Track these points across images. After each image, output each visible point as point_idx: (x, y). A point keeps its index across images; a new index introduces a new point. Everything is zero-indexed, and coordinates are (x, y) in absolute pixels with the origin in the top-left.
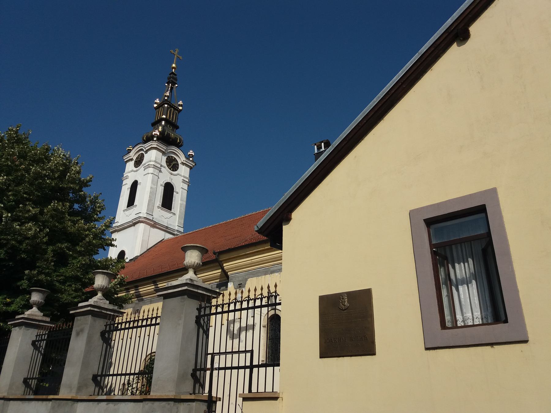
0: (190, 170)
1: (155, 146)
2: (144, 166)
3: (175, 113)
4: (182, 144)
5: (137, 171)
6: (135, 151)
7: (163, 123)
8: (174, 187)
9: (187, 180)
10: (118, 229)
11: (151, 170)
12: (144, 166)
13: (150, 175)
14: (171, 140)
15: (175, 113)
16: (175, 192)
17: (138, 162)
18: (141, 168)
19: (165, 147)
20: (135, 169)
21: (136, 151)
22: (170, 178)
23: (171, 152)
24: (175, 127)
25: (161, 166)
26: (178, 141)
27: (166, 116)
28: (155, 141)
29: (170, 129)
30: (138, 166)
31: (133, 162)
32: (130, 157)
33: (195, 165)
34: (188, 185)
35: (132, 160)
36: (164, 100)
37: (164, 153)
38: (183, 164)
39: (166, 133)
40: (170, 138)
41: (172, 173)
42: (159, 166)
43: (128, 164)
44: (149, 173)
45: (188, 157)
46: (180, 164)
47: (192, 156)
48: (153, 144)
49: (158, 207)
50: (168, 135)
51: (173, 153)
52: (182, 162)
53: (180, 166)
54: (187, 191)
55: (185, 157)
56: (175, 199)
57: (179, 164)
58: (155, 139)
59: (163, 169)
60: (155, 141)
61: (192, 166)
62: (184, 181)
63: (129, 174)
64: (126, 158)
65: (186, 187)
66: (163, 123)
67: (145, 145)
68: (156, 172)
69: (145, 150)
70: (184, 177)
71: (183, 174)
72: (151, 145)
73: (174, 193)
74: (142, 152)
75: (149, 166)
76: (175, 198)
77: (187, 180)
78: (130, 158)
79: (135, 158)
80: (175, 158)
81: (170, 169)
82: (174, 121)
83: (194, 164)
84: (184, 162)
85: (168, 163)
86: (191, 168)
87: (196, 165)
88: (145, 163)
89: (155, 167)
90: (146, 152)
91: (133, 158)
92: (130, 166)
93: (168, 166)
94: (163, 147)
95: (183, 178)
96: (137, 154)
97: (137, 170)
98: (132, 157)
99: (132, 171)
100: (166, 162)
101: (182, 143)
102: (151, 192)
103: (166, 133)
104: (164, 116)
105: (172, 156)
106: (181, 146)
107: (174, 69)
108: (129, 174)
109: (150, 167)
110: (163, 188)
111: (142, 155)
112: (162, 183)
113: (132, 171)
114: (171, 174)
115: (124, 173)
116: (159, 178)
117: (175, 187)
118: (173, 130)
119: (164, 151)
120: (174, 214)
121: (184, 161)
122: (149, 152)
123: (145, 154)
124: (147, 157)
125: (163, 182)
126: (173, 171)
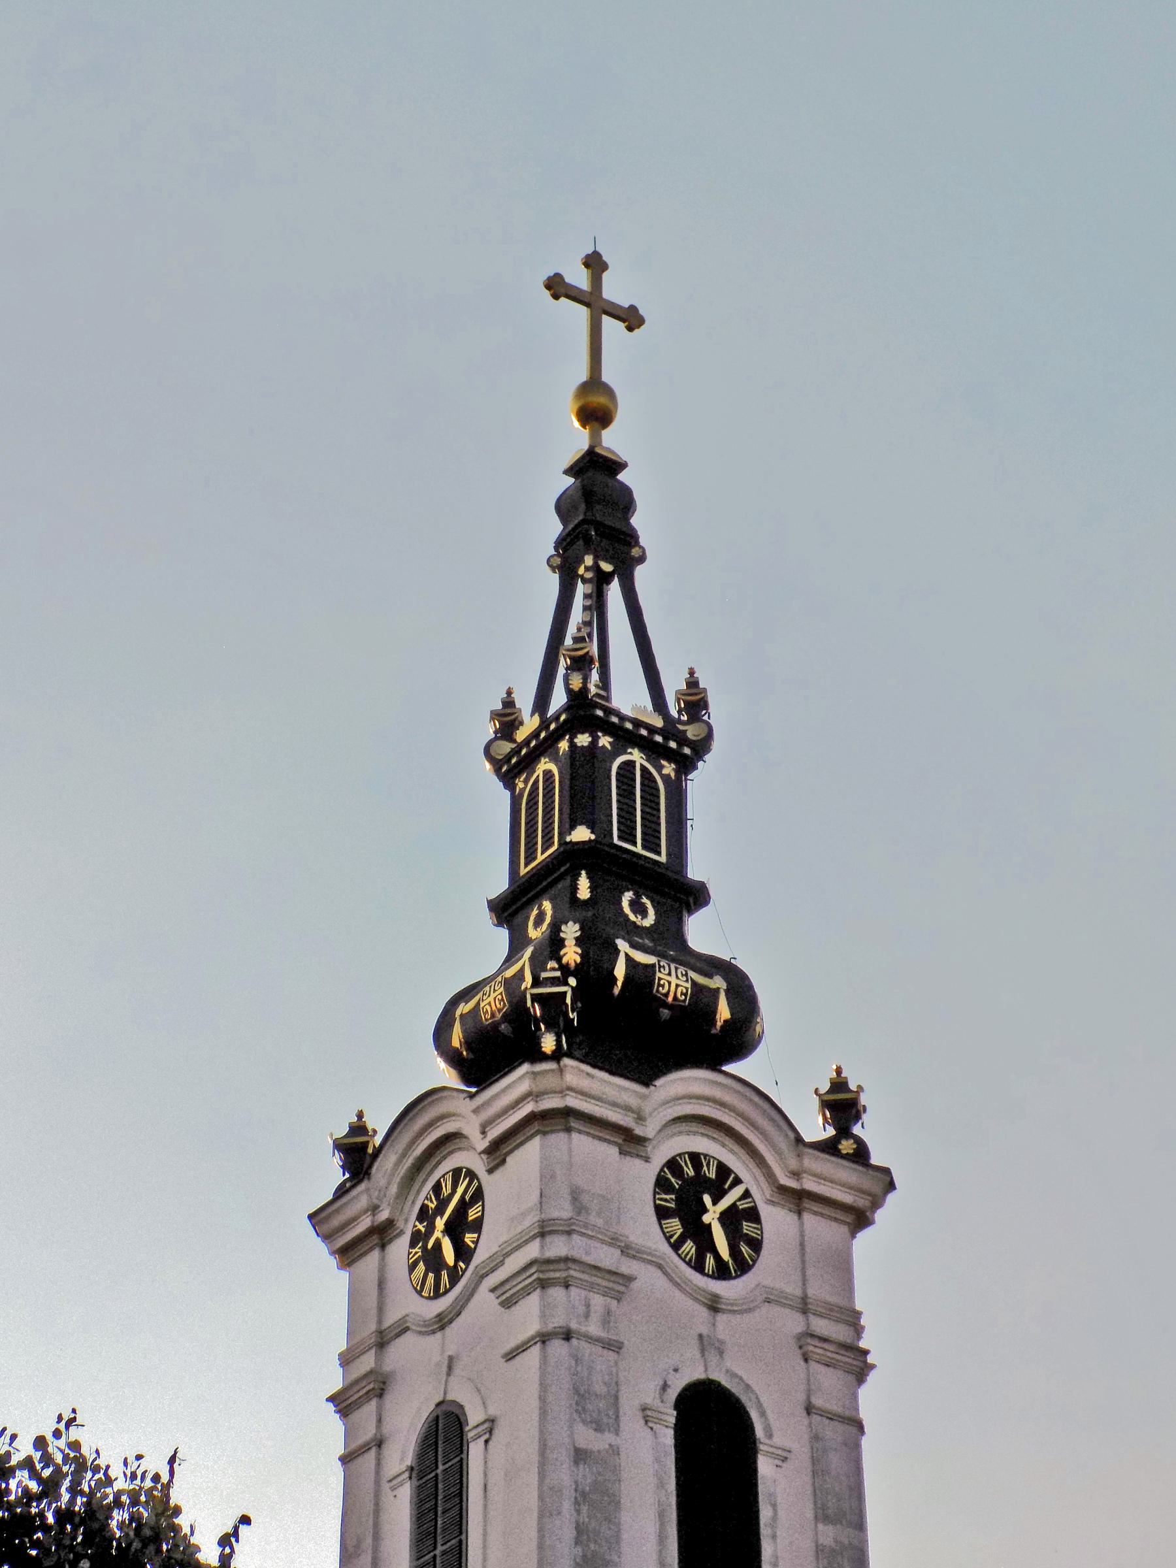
5: (442, 1322)
6: (404, 1155)
8: (754, 1415)
14: (665, 1013)
21: (409, 1161)
23: (684, 1127)
25: (628, 1251)
26: (724, 1012)
28: (557, 1055)
39: (620, 971)
46: (771, 1202)
51: (694, 1127)
52: (783, 1190)
56: (775, 1517)
57: (765, 1211)
58: (548, 1043)
60: (557, 1055)
69: (482, 1144)
73: (764, 1466)
76: (774, 1506)
88: (495, 1249)
96: (422, 1176)
97: (440, 1317)
100: (662, 1213)
102: (584, 1495)
103: (620, 971)
110: (668, 1437)
112: (651, 1398)
117: (763, 1414)
123: (490, 1171)
125: (665, 1387)
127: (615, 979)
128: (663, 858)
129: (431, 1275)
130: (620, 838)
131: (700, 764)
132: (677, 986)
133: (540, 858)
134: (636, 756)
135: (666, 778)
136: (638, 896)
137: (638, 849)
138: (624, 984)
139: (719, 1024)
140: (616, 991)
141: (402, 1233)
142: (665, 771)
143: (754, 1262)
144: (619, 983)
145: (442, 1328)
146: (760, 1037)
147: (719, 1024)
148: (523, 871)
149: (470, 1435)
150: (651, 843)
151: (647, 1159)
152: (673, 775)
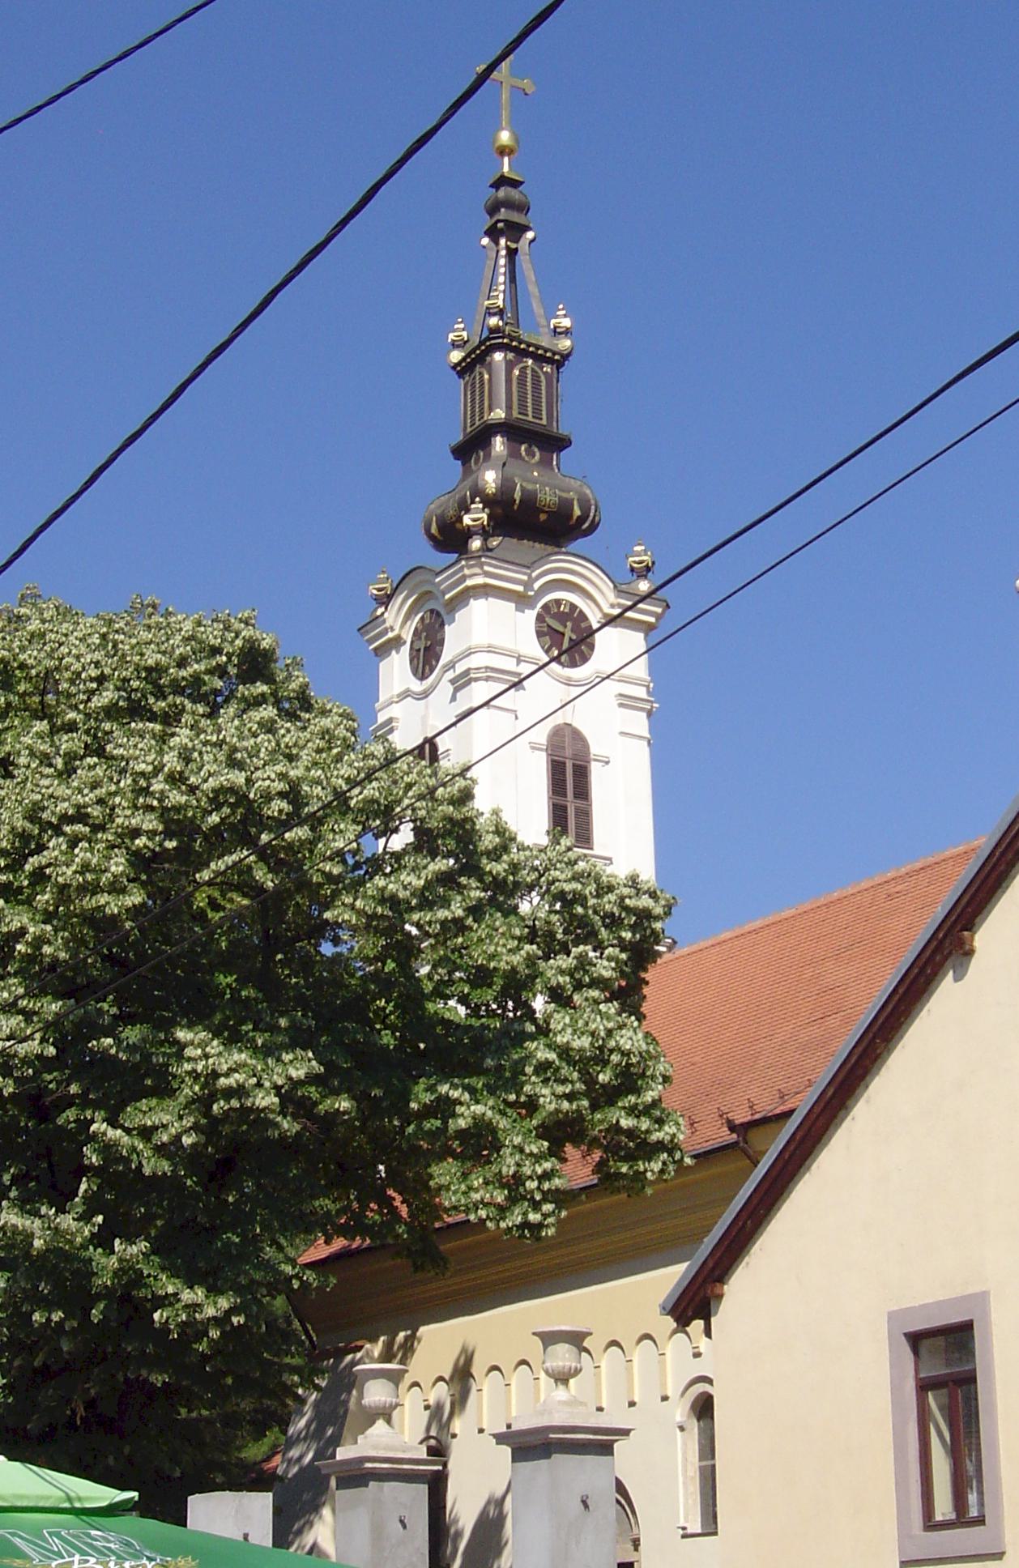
0: (646, 636)
2: (450, 675)
3: (543, 378)
5: (425, 695)
9: (641, 693)
12: (450, 675)
14: (543, 517)
15: (543, 378)
16: (595, 760)
17: (426, 657)
19: (525, 574)
20: (417, 686)
24: (552, 443)
26: (577, 512)
27: (509, 408)
29: (533, 461)
31: (405, 650)
33: (663, 612)
34: (650, 714)
35: (397, 642)
36: (485, 329)
37: (522, 601)
39: (517, 496)
41: (569, 679)
50: (529, 501)
61: (652, 620)
63: (394, 711)
65: (639, 723)
66: (499, 444)
77: (641, 693)
78: (390, 635)
79: (408, 636)
80: (573, 607)
82: (544, 422)
83: (659, 610)
88: (450, 658)
91: (404, 636)
94: (512, 578)
98: (396, 632)
101: (594, 516)
103: (517, 496)
104: (499, 414)
105: (558, 602)
106: (594, 527)
107: (506, 160)
108: (394, 711)
113: (406, 694)
118: (546, 463)
119: (520, 588)
126: (573, 664)
128: (544, 422)
131: (566, 363)
133: (477, 423)
134: (530, 362)
135: (546, 373)
136: (530, 446)
137: (530, 418)
138: (520, 501)
139: (575, 518)
140: (516, 507)
141: (405, 642)
142: (545, 369)
143: (591, 656)
144: (517, 502)
145: (426, 697)
146: (598, 523)
147: (575, 518)
148: (469, 430)
149: (441, 757)
150: (537, 413)
152: (549, 370)
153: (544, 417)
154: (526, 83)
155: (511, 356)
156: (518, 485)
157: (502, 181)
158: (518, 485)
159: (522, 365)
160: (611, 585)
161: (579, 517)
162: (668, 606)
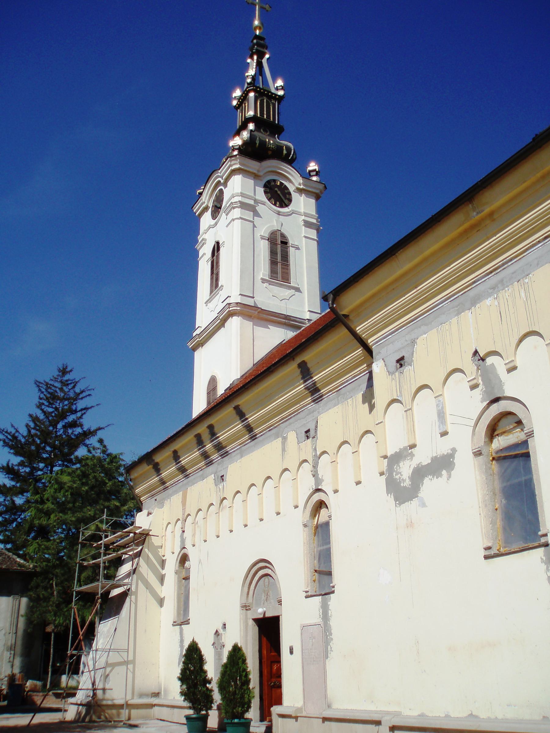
1: (237, 166)
4: (293, 156)
5: (216, 224)
7: (251, 126)
10: (201, 339)
11: (237, 213)
13: (238, 223)
16: (292, 247)
18: (223, 217)
20: (213, 222)
22: (277, 221)
25: (256, 201)
26: (285, 152)
30: (217, 215)
32: (202, 204)
35: (206, 209)
37: (255, 176)
38: (300, 191)
39: (258, 142)
40: (269, 149)
42: (252, 202)
43: (202, 220)
44: (233, 220)
45: (306, 176)
46: (294, 191)
47: (315, 172)
48: (233, 162)
49: (264, 281)
53: (295, 196)
54: (317, 242)
55: (301, 176)
57: (292, 193)
59: (260, 208)
61: (317, 191)
62: (308, 224)
64: (197, 209)
65: (313, 234)
66: (251, 126)
67: (219, 171)
68: (249, 215)
70: (306, 215)
71: (302, 211)
72: (230, 166)
74: (222, 187)
75: (232, 207)
78: (204, 206)
79: (210, 205)
81: (275, 205)
84: (302, 187)
85: (269, 194)
86: (317, 197)
87: (325, 187)
89: (243, 206)
90: (225, 184)
92: (206, 220)
93: (269, 200)
95: (303, 217)
99: (209, 228)
101: (293, 155)
103: (258, 142)
109: (234, 208)
111: (221, 191)
112: (262, 234)
113: (209, 228)
114: (279, 213)
115: (199, 237)
116: (254, 226)
120: (298, 290)
121: (300, 184)
122: (229, 183)
124: (227, 193)
126: (281, 206)
127: (256, 143)
129: (215, 214)
130: (260, 115)
131: (282, 101)
132: (273, 146)
139: (284, 154)
141: (210, 207)
144: (258, 144)
147: (284, 154)
151: (261, 180)
152: (274, 102)
153: (271, 119)
154: (267, 7)
155: (257, 94)
156: (258, 138)
157: (256, 37)
158: (258, 138)
159: (262, 98)
160: (299, 175)
161: (286, 154)
162: (325, 187)
